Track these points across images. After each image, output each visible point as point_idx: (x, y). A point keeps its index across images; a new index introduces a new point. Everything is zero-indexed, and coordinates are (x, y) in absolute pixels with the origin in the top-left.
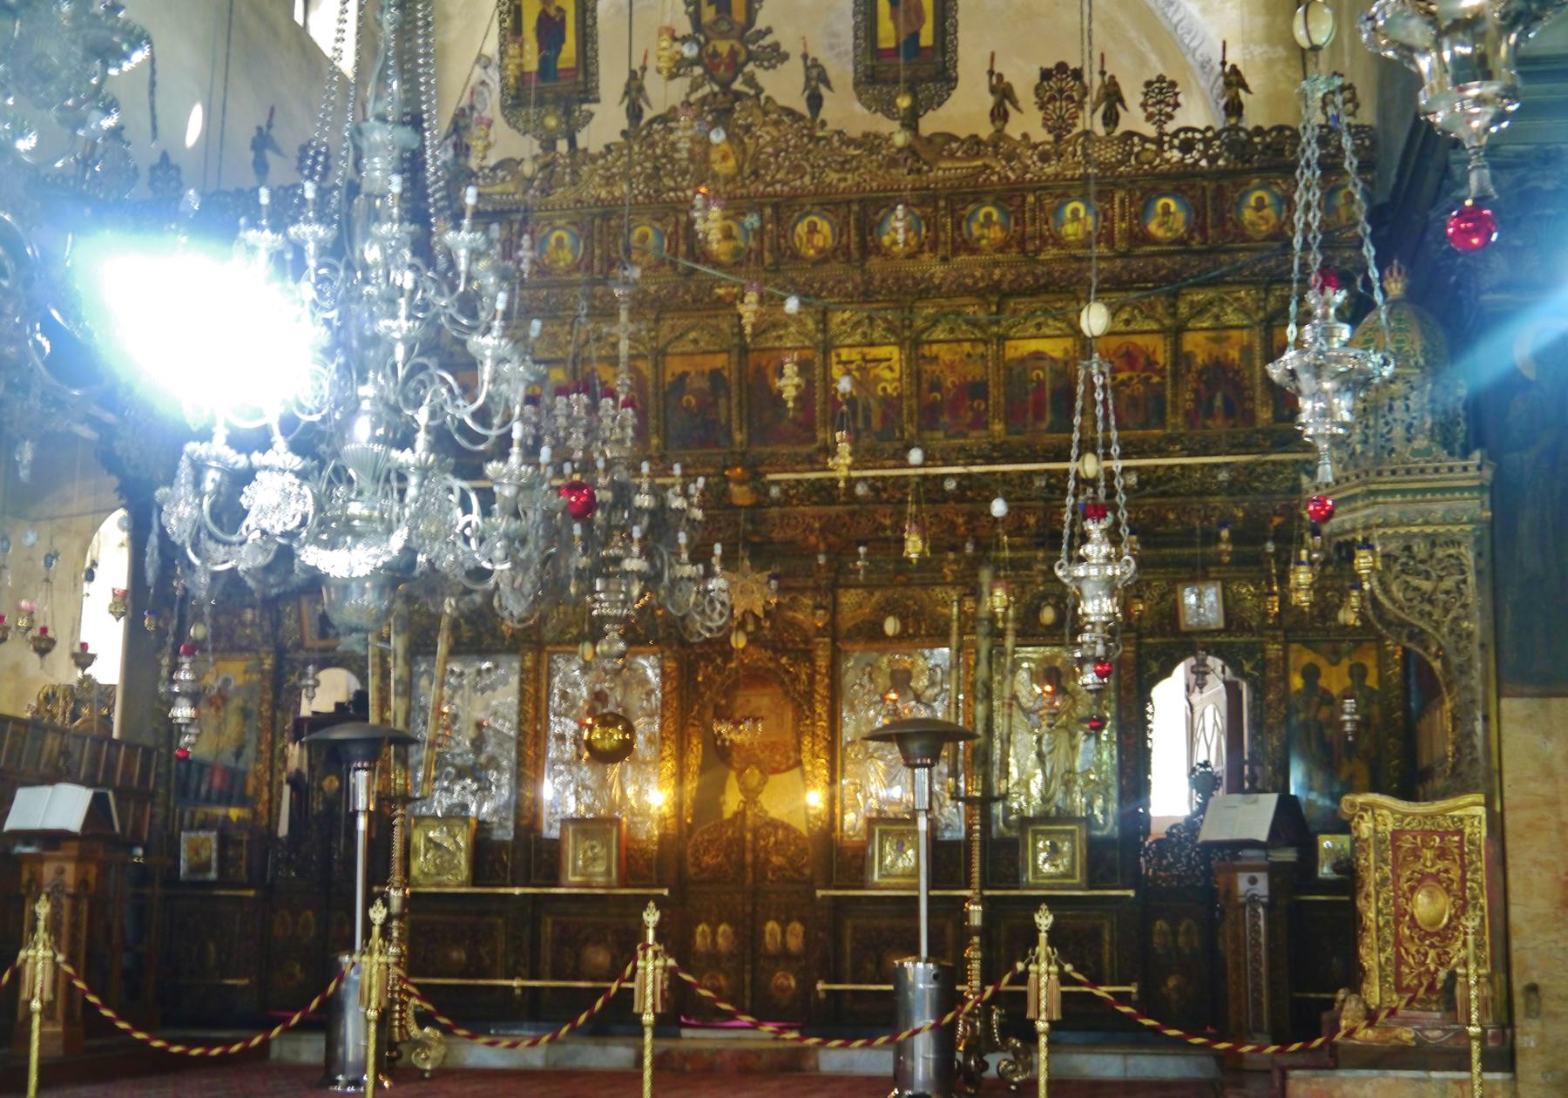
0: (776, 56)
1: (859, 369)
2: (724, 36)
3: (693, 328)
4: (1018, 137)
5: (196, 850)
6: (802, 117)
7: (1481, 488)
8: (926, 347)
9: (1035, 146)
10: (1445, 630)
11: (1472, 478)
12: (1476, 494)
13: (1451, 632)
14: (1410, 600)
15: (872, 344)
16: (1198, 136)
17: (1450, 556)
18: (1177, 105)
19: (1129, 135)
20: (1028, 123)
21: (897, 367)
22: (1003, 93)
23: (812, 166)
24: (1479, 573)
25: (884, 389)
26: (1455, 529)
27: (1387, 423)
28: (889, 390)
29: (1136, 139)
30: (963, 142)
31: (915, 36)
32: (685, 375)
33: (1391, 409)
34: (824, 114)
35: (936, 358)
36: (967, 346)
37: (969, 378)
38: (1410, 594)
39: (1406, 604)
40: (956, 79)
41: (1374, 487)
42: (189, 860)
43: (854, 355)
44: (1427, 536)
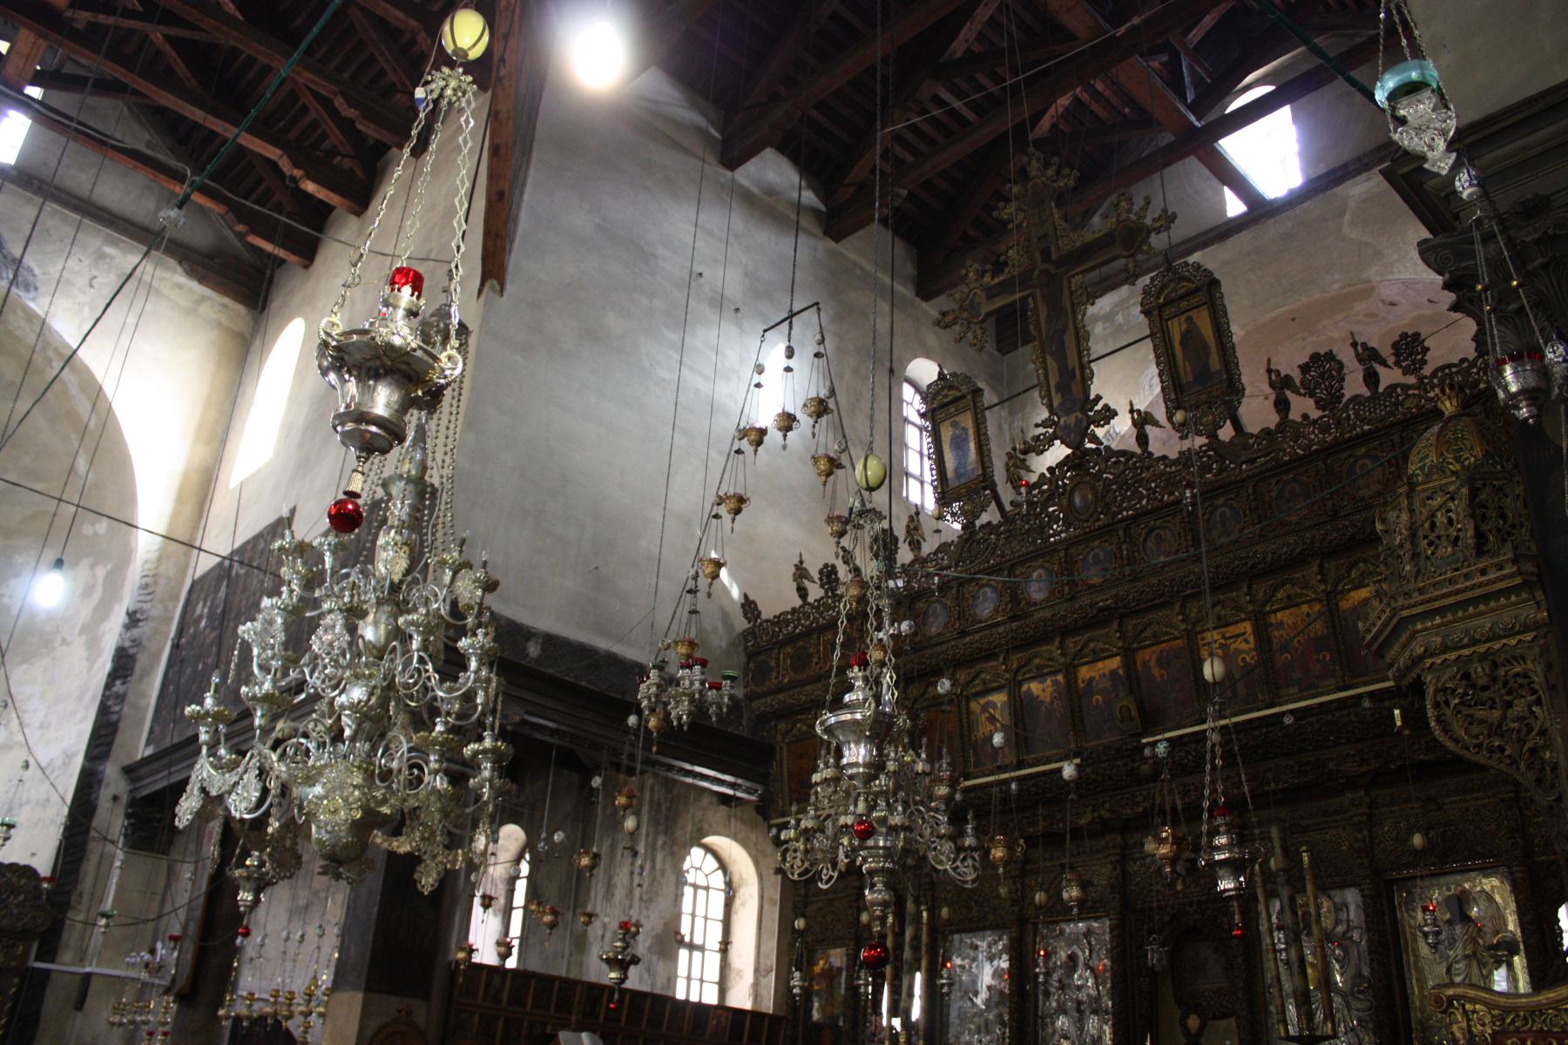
0: (1109, 414)
1: (1222, 646)
2: (1068, 412)
4: (1299, 420)
6: (1133, 454)
7: (1525, 584)
8: (1273, 616)
9: (1315, 422)
10: (1522, 766)
11: (1511, 576)
13: (1529, 767)
14: (1476, 737)
15: (1227, 625)
16: (1454, 370)
17: (1517, 675)
18: (1426, 350)
19: (1393, 387)
20: (1302, 406)
21: (1251, 639)
22: (1281, 384)
23: (1149, 489)
24: (1553, 688)
25: (1244, 660)
26: (1513, 642)
27: (1431, 544)
28: (1248, 659)
29: (1399, 390)
30: (1257, 437)
31: (1206, 366)
32: (1092, 679)
33: (1433, 526)
34: (1150, 449)
35: (1282, 623)
36: (1305, 608)
37: (1312, 635)
38: (1475, 729)
40: (1244, 389)
41: (1405, 613)
43: (1216, 635)
44: (1484, 656)
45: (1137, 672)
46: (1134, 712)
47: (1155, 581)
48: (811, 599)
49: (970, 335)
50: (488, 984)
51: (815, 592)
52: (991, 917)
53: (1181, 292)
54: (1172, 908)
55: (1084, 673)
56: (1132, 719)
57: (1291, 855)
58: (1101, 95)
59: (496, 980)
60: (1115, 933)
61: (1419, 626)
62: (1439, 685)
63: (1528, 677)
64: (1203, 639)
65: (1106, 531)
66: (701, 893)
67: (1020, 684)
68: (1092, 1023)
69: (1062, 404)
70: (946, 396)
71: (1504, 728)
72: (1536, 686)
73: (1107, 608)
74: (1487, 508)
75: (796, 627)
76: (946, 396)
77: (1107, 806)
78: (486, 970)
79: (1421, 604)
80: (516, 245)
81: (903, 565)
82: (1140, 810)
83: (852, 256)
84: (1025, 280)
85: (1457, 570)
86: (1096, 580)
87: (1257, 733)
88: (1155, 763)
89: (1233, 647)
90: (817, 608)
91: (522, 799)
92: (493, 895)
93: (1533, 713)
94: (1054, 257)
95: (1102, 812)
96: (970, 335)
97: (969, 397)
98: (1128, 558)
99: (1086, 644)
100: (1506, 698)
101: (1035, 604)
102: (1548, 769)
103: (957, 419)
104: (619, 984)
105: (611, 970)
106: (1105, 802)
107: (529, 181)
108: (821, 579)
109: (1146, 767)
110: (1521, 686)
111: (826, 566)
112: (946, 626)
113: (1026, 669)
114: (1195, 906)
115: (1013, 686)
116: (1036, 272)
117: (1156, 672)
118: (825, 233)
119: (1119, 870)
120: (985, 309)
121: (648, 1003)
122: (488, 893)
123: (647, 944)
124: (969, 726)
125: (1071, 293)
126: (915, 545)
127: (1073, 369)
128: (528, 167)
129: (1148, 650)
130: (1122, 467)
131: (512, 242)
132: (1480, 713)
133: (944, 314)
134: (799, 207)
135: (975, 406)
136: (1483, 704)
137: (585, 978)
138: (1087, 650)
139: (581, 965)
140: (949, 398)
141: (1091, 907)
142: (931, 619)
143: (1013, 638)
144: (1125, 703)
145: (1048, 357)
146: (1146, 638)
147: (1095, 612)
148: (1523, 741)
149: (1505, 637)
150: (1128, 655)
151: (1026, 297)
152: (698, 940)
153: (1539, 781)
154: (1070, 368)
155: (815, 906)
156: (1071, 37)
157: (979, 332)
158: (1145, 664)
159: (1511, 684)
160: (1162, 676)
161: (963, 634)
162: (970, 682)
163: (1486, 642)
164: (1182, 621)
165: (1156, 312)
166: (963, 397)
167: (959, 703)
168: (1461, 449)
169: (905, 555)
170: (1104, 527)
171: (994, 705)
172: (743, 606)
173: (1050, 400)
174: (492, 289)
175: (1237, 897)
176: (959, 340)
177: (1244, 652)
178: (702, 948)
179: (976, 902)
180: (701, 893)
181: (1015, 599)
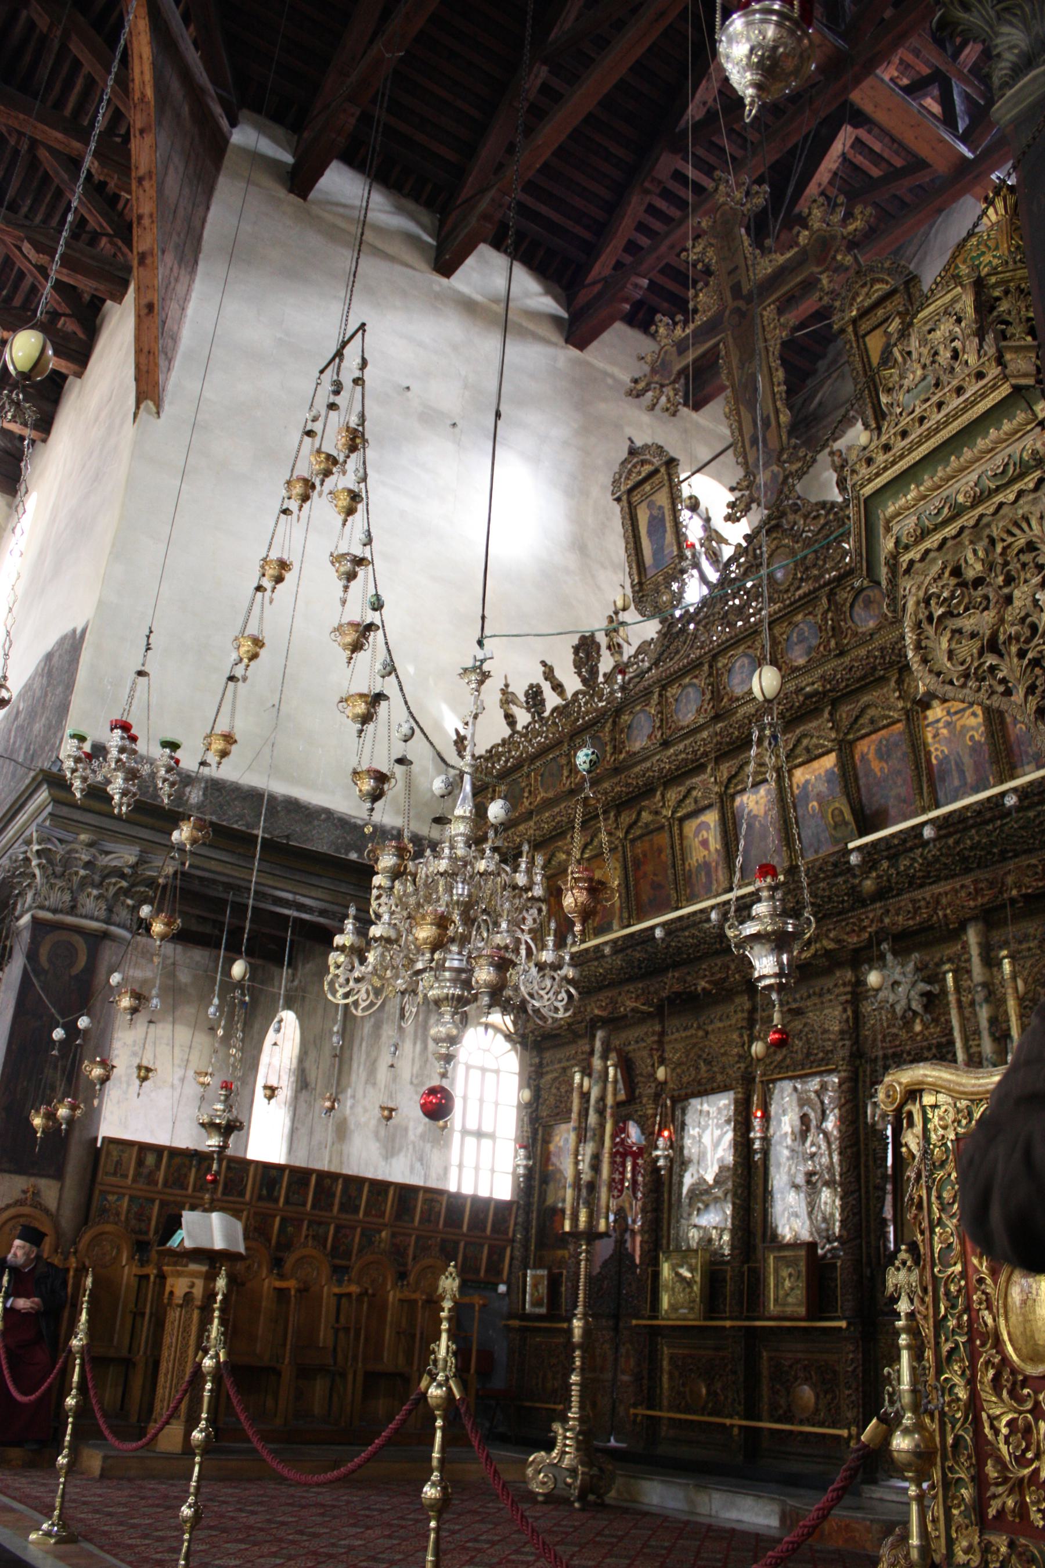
1: (948, 724)
3: (805, 736)
5: (535, 1286)
12: (1021, 416)
25: (972, 738)
28: (977, 737)
32: (807, 782)
41: (868, 490)
42: (532, 1295)
45: (854, 767)
46: (848, 816)
47: (863, 652)
48: (519, 727)
49: (663, 399)
50: (140, 1163)
51: (523, 718)
52: (719, 1077)
54: (909, 1053)
55: (800, 775)
56: (847, 824)
57: (991, 962)
58: (879, 156)
59: (150, 1159)
60: (844, 1087)
61: (891, 510)
62: (921, 594)
63: (1037, 549)
64: (926, 718)
65: (809, 601)
66: (490, 1077)
67: (733, 797)
68: (826, 1194)
70: (639, 473)
71: (1002, 638)
73: (816, 693)
75: (507, 761)
76: (639, 473)
77: (831, 935)
78: (136, 1149)
79: (885, 469)
80: (177, 363)
81: (605, 675)
82: (867, 935)
83: (601, 365)
86: (801, 661)
87: (990, 827)
88: (879, 877)
89: (959, 724)
90: (525, 735)
91: (296, 983)
92: (151, 1066)
94: (745, 292)
95: (825, 942)
96: (663, 399)
97: (663, 470)
98: (833, 628)
99: (799, 741)
100: (1006, 591)
101: (738, 699)
103: (653, 498)
104: (219, 1153)
105: (209, 1137)
106: (829, 930)
107: (194, 295)
108: (527, 703)
109: (868, 883)
110: (1024, 565)
111: (531, 686)
112: (649, 737)
113: (739, 778)
114: (934, 1051)
115: (725, 802)
116: (727, 313)
117: (876, 766)
118: (568, 340)
119: (849, 1013)
120: (677, 367)
121: (340, 1187)
122: (145, 1063)
123: (420, 1129)
124: (682, 854)
126: (615, 648)
127: (768, 417)
128: (192, 280)
130: (822, 521)
131: (170, 361)
132: (967, 623)
133: (636, 381)
134: (535, 315)
135: (670, 480)
137: (346, 1171)
138: (798, 751)
139: (341, 1154)
140: (643, 474)
141: (822, 1059)
142: (636, 732)
143: (718, 743)
144: (837, 805)
145: (742, 408)
146: (863, 726)
147: (801, 698)
149: (998, 489)
150: (845, 749)
151: (717, 345)
152: (487, 1128)
155: (549, 1077)
157: (671, 394)
158: (863, 757)
159: (1014, 566)
160: (882, 769)
161: (666, 744)
162: (681, 801)
163: (973, 506)
164: (898, 698)
165: (850, 329)
166: (656, 471)
167: (670, 826)
169: (606, 663)
170: (805, 595)
171: (705, 825)
172: (456, 743)
173: (745, 457)
174: (148, 411)
175: (780, 988)
176: (652, 408)
177: (973, 728)
178: (492, 1136)
179: (705, 1060)
180: (490, 1077)
181: (717, 696)
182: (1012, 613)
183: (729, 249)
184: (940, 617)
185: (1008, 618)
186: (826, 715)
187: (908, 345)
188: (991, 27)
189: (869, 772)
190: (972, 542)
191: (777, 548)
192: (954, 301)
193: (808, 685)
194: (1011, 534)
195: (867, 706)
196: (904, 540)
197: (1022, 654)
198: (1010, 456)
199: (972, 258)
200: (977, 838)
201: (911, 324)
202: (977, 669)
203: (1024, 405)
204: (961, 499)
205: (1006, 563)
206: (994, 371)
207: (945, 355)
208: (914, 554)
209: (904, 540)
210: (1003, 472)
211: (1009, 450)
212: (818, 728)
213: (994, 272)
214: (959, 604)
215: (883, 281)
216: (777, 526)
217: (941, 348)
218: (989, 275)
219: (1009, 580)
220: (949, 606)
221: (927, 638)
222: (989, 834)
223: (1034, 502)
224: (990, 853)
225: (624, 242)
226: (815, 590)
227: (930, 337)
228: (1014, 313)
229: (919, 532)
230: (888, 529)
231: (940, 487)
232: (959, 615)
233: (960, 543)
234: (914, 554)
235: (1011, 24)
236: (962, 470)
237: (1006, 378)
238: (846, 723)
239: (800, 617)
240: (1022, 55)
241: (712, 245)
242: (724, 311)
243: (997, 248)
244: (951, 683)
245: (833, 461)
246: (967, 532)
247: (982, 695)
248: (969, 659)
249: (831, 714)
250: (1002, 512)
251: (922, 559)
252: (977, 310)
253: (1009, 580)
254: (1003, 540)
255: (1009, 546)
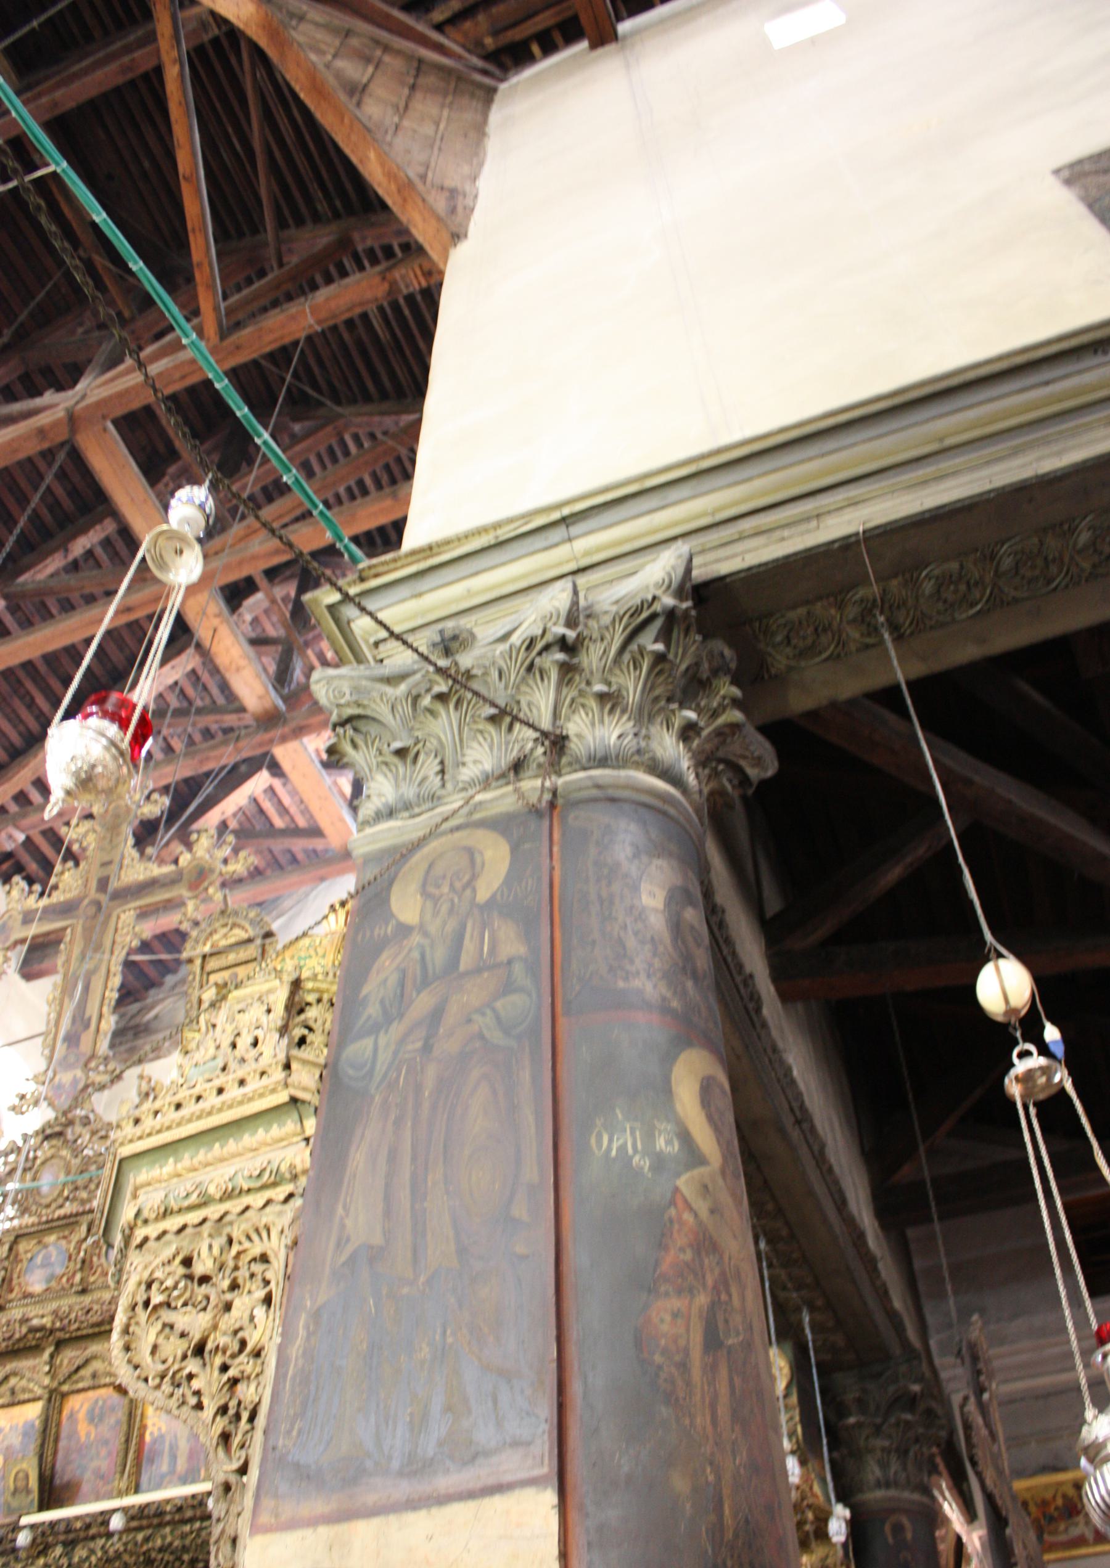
3: (14, 1373)
39: (152, 1367)
41: (126, 1151)
45: (59, 1425)
53: (232, 940)
69: (65, 1058)
71: (210, 1346)
72: (269, 1275)
73: (42, 1328)
74: (311, 1029)
84: (67, 909)
85: (210, 1080)
86: (37, 1288)
93: (252, 1318)
98: (83, 1262)
100: (228, 1296)
102: (245, 1416)
116: (86, 901)
120: (17, 935)
125: (116, 930)
127: (90, 1019)
129: (80, 1397)
136: (194, 1305)
146: (82, 1379)
147: (24, 1330)
148: (224, 1368)
150: (55, 1398)
151: (64, 929)
153: (225, 1438)
154: (87, 1016)
156: (242, 709)
158: (72, 1415)
160: (88, 1434)
163: (221, 1200)
165: (198, 962)
168: (310, 957)
170: (65, 1217)
182: (228, 1322)
183: (111, 841)
184: (155, 1308)
185: (222, 1326)
186: (46, 1355)
187: (216, 1017)
188: (370, 770)
189: (74, 1433)
190: (210, 1236)
191: (52, 1157)
192: (270, 991)
193: (36, 1316)
194: (249, 1238)
195: (94, 1357)
196: (145, 1214)
197: (224, 1368)
198: (269, 1162)
199: (300, 958)
200: (169, 1539)
201: (224, 998)
202: (174, 1374)
203: (296, 1116)
204: (212, 1190)
205: (236, 1268)
206: (279, 1075)
207: (244, 1042)
208: (152, 1231)
209: (145, 1214)
210: (259, 1176)
211: (270, 1156)
212: (33, 1369)
213: (314, 977)
214: (179, 1297)
215: (243, 928)
216: (60, 1134)
217: (244, 1033)
218: (308, 979)
219: (234, 1286)
220: (169, 1296)
221: (137, 1323)
222: (183, 1536)
223: (280, 1214)
224: (179, 1558)
225: (16, 790)
226: (77, 1214)
227: (238, 1017)
228: (320, 1022)
229: (162, 1210)
230: (135, 1196)
231: (195, 1170)
232: (176, 1308)
233: (199, 1234)
234: (152, 1231)
235: (386, 776)
236: (222, 1160)
237: (286, 1085)
238: (64, 1371)
239: (52, 1238)
240: (386, 805)
241: (94, 831)
242: (85, 896)
243: (324, 956)
244: (146, 1380)
245: (140, 1086)
246: (208, 1225)
247: (173, 1403)
248: (170, 1360)
249: (52, 1356)
250: (248, 1214)
251: (159, 1238)
252: (288, 1008)
253: (234, 1286)
254: (240, 1243)
255: (244, 1251)
